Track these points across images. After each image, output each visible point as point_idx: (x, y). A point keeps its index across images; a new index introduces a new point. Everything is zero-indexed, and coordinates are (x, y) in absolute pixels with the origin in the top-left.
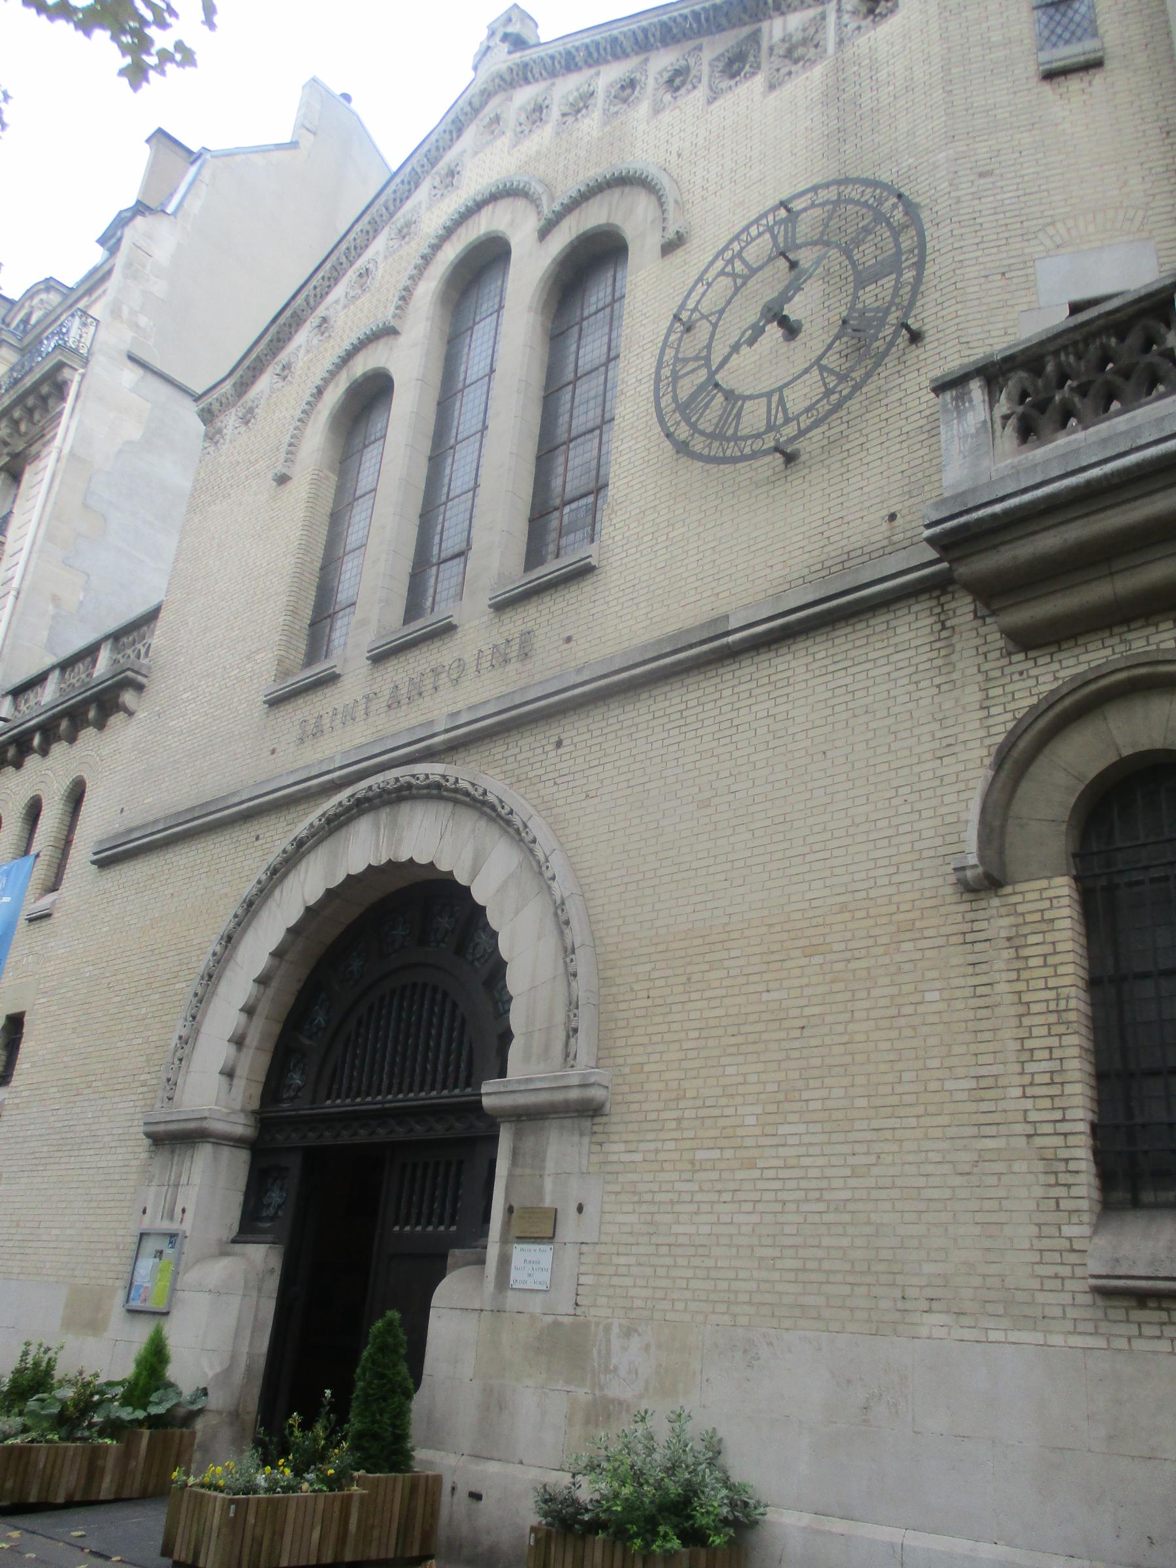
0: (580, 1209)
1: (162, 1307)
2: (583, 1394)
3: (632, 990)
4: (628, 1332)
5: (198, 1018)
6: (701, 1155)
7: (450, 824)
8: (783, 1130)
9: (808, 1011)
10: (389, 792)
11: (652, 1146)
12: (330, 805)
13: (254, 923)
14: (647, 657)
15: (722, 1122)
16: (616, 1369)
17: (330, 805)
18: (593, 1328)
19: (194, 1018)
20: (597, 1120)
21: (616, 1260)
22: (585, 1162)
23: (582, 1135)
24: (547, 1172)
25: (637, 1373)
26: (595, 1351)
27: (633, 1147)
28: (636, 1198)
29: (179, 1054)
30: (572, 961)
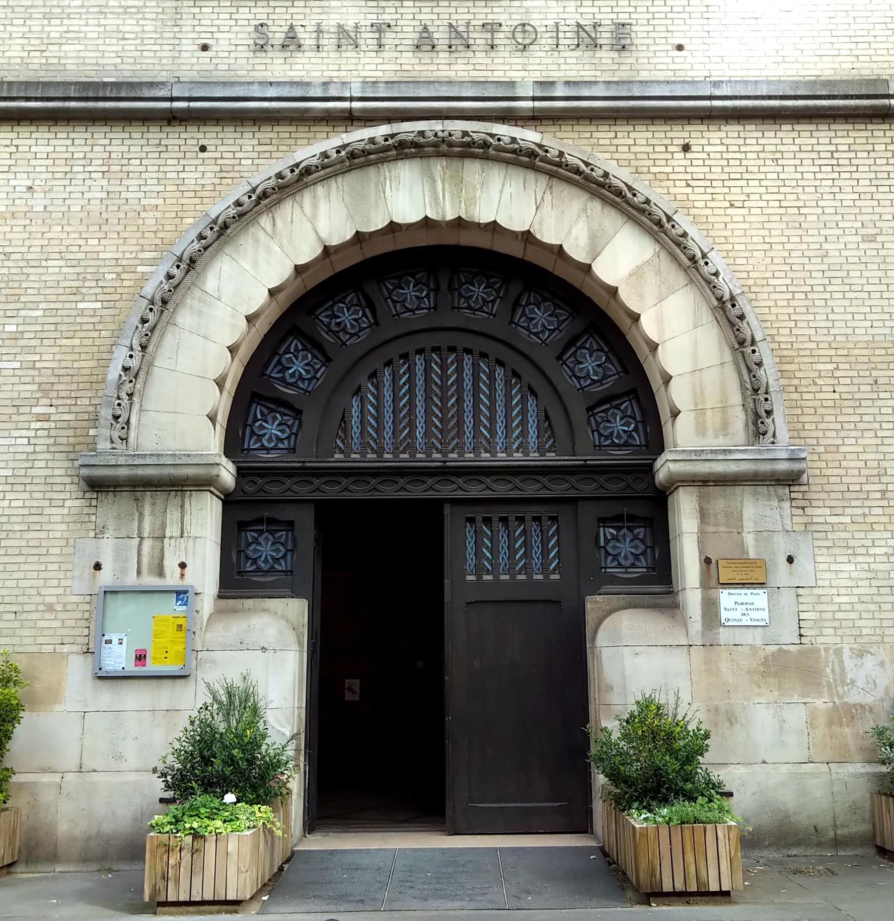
0: (790, 560)
2: (821, 703)
3: (815, 384)
4: (861, 654)
5: (150, 349)
7: (548, 197)
10: (451, 145)
11: (859, 511)
12: (359, 135)
13: (228, 250)
14: (799, 93)
16: (853, 682)
17: (359, 135)
18: (823, 652)
19: (144, 348)
20: (793, 488)
21: (837, 599)
22: (789, 523)
23: (781, 500)
24: (745, 530)
25: (875, 683)
26: (828, 670)
27: (839, 511)
28: (850, 551)
29: (127, 387)
30: (754, 351)
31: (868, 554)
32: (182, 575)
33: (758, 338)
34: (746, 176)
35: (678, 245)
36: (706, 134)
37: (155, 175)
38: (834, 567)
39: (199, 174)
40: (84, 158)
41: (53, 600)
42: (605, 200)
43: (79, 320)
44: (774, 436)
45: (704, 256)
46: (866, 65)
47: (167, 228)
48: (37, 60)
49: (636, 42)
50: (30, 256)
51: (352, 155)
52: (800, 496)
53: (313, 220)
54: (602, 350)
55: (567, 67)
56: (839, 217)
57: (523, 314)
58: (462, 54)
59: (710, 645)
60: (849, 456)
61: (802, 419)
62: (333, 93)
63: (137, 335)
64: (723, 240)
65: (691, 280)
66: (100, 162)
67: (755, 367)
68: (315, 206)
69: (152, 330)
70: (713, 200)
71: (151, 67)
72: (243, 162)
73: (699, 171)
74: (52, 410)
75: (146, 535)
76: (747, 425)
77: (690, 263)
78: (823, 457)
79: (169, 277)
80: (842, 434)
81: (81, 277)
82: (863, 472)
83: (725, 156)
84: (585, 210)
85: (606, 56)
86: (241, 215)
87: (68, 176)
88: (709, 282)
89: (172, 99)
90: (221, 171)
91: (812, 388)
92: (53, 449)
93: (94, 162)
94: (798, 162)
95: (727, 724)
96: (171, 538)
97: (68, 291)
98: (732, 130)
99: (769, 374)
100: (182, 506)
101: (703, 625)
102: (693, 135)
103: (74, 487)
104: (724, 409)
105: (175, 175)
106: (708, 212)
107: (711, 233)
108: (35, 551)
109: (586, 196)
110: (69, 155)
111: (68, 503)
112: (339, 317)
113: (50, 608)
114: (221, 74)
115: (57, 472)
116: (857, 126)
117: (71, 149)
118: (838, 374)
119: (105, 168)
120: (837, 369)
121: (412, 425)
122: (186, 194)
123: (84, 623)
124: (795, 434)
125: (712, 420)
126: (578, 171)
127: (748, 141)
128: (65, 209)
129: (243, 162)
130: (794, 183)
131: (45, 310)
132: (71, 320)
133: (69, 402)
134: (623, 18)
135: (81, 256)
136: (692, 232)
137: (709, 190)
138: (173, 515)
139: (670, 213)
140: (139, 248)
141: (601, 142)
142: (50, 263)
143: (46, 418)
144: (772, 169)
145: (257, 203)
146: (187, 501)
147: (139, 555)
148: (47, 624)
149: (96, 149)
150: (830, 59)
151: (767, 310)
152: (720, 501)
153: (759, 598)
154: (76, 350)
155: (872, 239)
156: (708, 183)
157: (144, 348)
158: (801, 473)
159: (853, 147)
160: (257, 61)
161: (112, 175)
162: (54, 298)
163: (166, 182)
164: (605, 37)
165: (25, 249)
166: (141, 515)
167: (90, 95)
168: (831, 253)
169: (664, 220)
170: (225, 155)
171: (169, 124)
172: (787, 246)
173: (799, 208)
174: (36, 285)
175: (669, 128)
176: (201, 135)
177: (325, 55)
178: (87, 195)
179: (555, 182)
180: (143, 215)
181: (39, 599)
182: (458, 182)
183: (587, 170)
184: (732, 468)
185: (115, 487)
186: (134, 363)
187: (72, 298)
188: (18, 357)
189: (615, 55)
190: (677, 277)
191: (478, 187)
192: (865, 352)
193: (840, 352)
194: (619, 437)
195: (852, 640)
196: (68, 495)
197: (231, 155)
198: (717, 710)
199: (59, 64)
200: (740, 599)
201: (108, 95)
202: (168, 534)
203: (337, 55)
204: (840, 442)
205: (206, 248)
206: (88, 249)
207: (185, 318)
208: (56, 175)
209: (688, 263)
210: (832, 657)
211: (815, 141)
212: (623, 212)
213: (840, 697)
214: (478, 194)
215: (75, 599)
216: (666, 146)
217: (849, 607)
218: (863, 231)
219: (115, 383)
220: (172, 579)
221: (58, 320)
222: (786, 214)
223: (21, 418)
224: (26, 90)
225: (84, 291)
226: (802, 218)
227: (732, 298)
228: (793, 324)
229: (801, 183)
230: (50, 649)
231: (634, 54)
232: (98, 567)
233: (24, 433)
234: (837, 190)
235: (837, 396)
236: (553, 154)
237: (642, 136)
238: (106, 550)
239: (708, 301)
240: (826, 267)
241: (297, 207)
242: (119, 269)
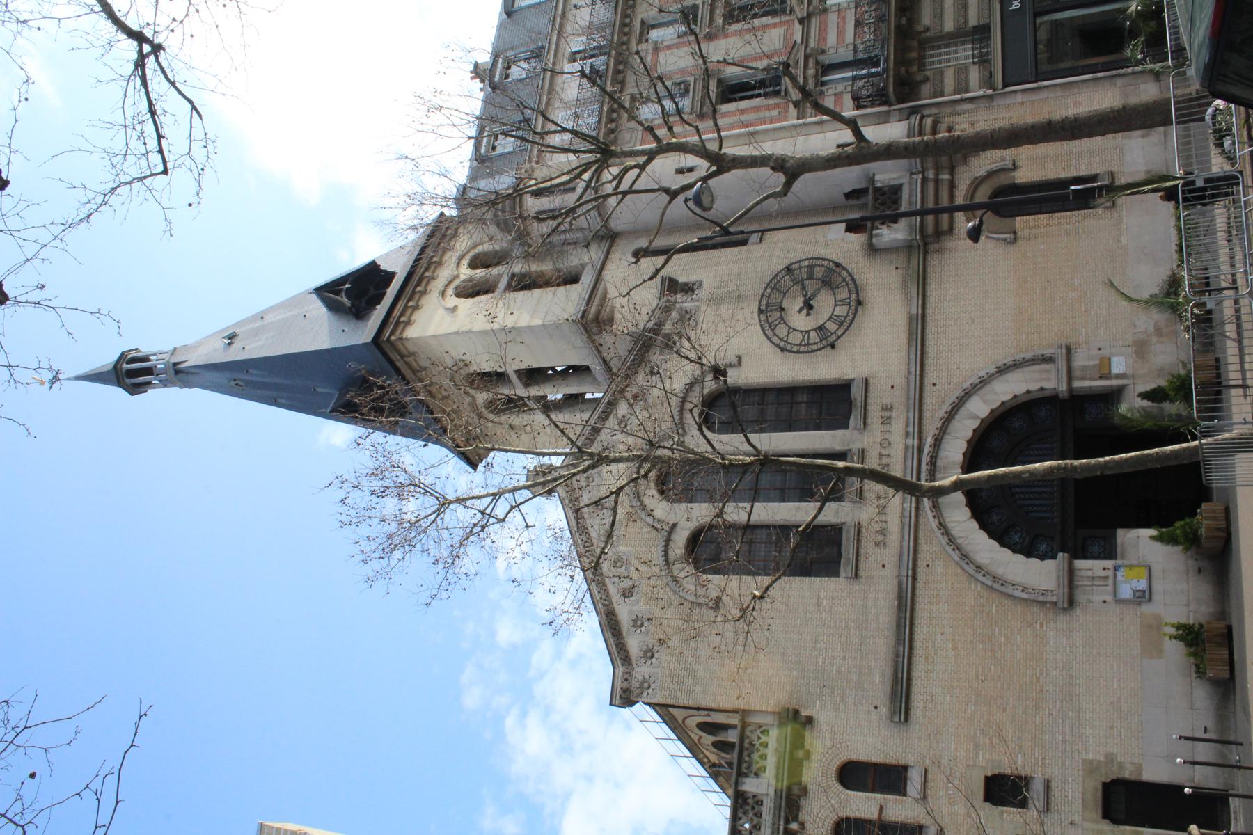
2: (1154, 339)
4: (1135, 326)
39: (939, 567)
48: (886, 633)
59: (1133, 377)
77: (983, 382)
85: (894, 414)
98: (927, 368)
99: (1028, 356)
114: (895, 559)
121: (1041, 493)
134: (879, 407)
138: (1083, 573)
143: (1042, 625)
152: (1077, 373)
153: (1114, 360)
155: (973, 321)
164: (887, 414)
184: (1065, 369)
190: (988, 387)
207: (1000, 571)
220: (1110, 573)
237: (929, 401)
238: (1097, 598)
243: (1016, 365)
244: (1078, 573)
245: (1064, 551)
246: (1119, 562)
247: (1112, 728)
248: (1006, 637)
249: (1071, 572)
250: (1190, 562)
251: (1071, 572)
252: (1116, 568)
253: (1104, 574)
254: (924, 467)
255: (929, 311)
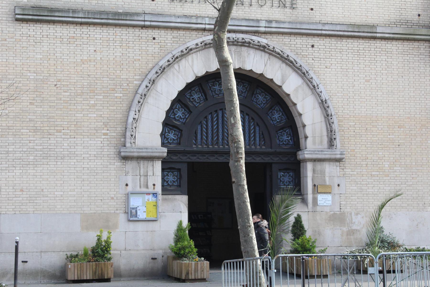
0: (339, 185)
1: (154, 219)
2: (345, 229)
3: (349, 129)
4: (357, 214)
6: (373, 173)
7: (269, 62)
8: (395, 168)
9: (400, 141)
10: (238, 42)
11: (359, 170)
15: (379, 166)
16: (354, 223)
19: (139, 111)
20: (341, 163)
23: (337, 166)
26: (348, 219)
27: (353, 170)
28: (356, 183)
29: (135, 125)
31: (361, 184)
32: (154, 188)
33: (333, 114)
34: (331, 57)
35: (310, 81)
36: (319, 42)
37: (138, 48)
38: (351, 188)
39: (153, 48)
40: (113, 40)
41: (113, 196)
42: (287, 64)
43: (115, 100)
44: (336, 146)
45: (318, 86)
46: (370, 20)
47: (143, 68)
49: (298, 6)
50: (97, 76)
51: (206, 44)
52: (342, 165)
53: (192, 67)
54: (281, 111)
55: (275, 14)
56: (359, 73)
57: (255, 97)
58: (241, 8)
60: (357, 153)
61: (344, 141)
62: (199, 21)
63: (137, 107)
64: (323, 79)
65: (313, 93)
66: (119, 42)
67: (331, 124)
68: (193, 61)
69: (141, 105)
70: (321, 65)
71: (134, 6)
72: (168, 44)
73: (316, 55)
74: (108, 132)
75: (142, 174)
76: (328, 142)
77: (314, 88)
78: (350, 153)
79: (147, 87)
80: (356, 146)
81: (115, 84)
82: (361, 158)
83: (325, 50)
84: (280, 67)
85: (288, 10)
86: (169, 65)
87: (108, 47)
88: (318, 95)
89: (144, 21)
90: (161, 47)
91: (348, 131)
92: (109, 145)
93: (117, 42)
94: (347, 53)
95: (318, 235)
96: (150, 176)
97: (111, 89)
98: (328, 40)
99: (335, 126)
100: (153, 165)
101: (313, 205)
102: (315, 42)
103: (117, 159)
104: (321, 137)
105: (145, 48)
106: (319, 69)
107: (320, 77)
108: (106, 180)
109: (281, 62)
110: (108, 39)
111: (116, 164)
112: (193, 96)
113: (112, 198)
114: (159, 10)
115: (111, 153)
116: (366, 41)
117: (109, 37)
118: (356, 126)
119: (121, 45)
120: (355, 124)
121: (218, 135)
122: (149, 55)
123: (124, 203)
124: (342, 145)
125: (317, 140)
126: (279, 54)
127: (332, 45)
128: (108, 59)
129: (168, 44)
130: (346, 60)
131: (103, 96)
132: (113, 100)
133: (114, 129)
135: (114, 77)
136: (314, 78)
137: (320, 62)
138: (150, 168)
139: (308, 70)
140: (134, 75)
141: (286, 43)
142: (104, 79)
143: (105, 134)
144: (339, 55)
145: (175, 61)
146: (154, 163)
147: (140, 181)
148: (111, 204)
149: (117, 37)
150: (359, 17)
151: (335, 104)
152: (319, 166)
153: (329, 197)
154: (115, 111)
156: (319, 59)
157: (139, 111)
158: (343, 159)
159: (364, 49)
160: (171, 6)
161: (123, 47)
162: (106, 92)
163: (142, 50)
165: (95, 74)
166: (140, 168)
167: (117, 18)
168: (356, 85)
169: (306, 73)
170: (162, 41)
171: (142, 29)
172: (343, 82)
173: (347, 69)
174: (100, 87)
175: (307, 39)
176: (153, 34)
177: (194, 5)
178: (115, 54)
179: (271, 56)
180: (135, 62)
181: (109, 195)
182: (240, 55)
183: (282, 54)
184: (323, 157)
185: (131, 158)
186: (136, 117)
187: (112, 92)
188: (96, 113)
189: (291, 11)
190: (308, 91)
191: (246, 57)
192: (364, 119)
193: (357, 119)
194: (285, 141)
195: (355, 210)
196: (115, 161)
197: (164, 41)
198: (315, 231)
199: (102, 3)
200: (323, 197)
201: (123, 18)
202: (149, 175)
203: (198, 5)
204: (355, 148)
205: (158, 76)
206: (117, 74)
207: (150, 100)
208: (104, 46)
209: (312, 87)
210: (349, 215)
211: (353, 46)
212: (292, 68)
213: (350, 227)
214: (246, 59)
215: (120, 195)
216: (307, 45)
217: (354, 200)
218: (366, 78)
219: (131, 124)
220: (151, 190)
221: (108, 100)
222: (343, 71)
223: (98, 134)
224: (94, 15)
225: (116, 89)
226: (348, 73)
227: (326, 100)
228: (343, 109)
229: (348, 61)
230: (113, 211)
231: (297, 11)
232: (127, 185)
233: (99, 139)
234: (359, 63)
235: (355, 133)
236: (271, 48)
237: (299, 41)
239: (318, 100)
240: (354, 90)
241: (186, 61)
242: (128, 82)
243: (327, 116)
244: (150, 163)
245: (169, 152)
246: (160, 197)
247: (22, 190)
248: (94, 105)
249: (151, 159)
250: (161, 252)
251: (151, 159)
252: (155, 195)
253: (150, 185)
254: (240, 36)
255: (378, 43)
